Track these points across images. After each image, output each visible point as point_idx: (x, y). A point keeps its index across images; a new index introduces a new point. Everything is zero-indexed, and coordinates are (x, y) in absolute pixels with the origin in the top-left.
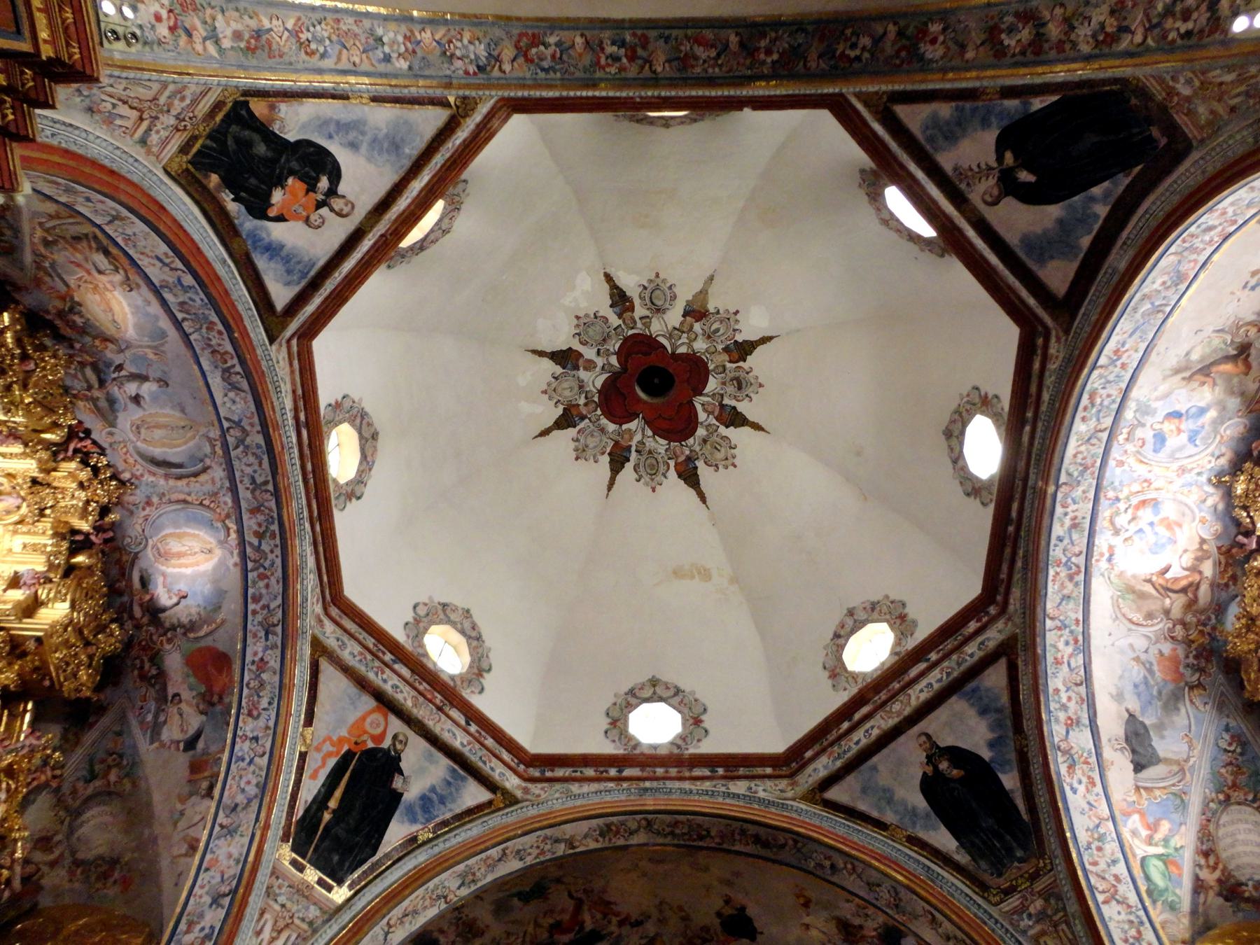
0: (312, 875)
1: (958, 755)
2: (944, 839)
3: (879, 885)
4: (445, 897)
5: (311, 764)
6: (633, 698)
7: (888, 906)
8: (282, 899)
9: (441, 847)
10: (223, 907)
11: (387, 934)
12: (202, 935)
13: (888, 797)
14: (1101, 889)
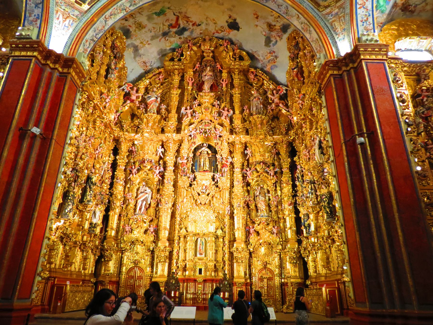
3: (282, 6)
4: (125, 10)
7: (283, 13)
8: (63, 7)
10: (40, 8)
11: (106, 21)
12: (35, 17)
14: (359, 3)
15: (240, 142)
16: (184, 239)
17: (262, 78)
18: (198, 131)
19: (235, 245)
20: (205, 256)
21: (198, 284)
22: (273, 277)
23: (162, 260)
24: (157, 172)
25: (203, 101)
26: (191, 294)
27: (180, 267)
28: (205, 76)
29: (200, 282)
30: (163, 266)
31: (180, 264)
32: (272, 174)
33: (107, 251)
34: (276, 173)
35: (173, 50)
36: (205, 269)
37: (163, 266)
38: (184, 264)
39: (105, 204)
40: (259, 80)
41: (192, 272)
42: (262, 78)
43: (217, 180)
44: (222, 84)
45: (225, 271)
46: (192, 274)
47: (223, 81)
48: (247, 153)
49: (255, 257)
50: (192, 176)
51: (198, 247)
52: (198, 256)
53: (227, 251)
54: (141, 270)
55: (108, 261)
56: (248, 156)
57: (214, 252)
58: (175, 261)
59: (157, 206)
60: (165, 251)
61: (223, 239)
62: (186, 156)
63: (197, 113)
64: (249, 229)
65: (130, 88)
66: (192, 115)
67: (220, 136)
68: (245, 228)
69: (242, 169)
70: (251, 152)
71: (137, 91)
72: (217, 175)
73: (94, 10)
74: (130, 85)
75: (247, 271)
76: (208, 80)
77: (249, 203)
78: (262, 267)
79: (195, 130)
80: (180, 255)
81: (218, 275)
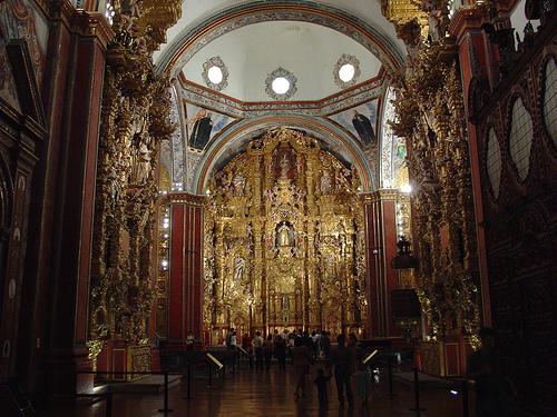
0: (196, 150)
1: (362, 117)
2: (356, 134)
5: (189, 125)
6: (274, 76)
9: (225, 135)
13: (344, 121)
35: (255, 138)
72: (295, 249)
73: (208, 154)
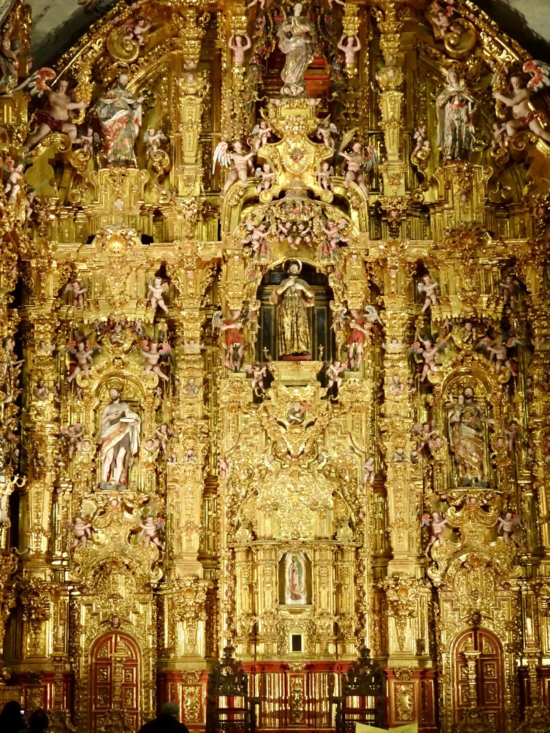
15: (403, 260)
16: (247, 556)
17: (476, 27)
18: (273, 229)
19: (391, 569)
20: (309, 602)
21: (291, 677)
22: (497, 655)
23: (188, 616)
24: (154, 358)
25: (281, 126)
26: (274, 701)
27: (239, 631)
28: (289, 35)
29: (297, 671)
30: (192, 629)
31: (238, 624)
32: (499, 357)
33: (37, 595)
34: (511, 352)
36: (310, 637)
37: (192, 629)
38: (252, 624)
39: (13, 463)
40: (465, 31)
41: (275, 645)
42: (476, 27)
43: (335, 383)
44: (342, 53)
45: (363, 641)
46: (275, 651)
47: (345, 43)
48: (424, 293)
49: (446, 601)
50: (259, 373)
51: (287, 577)
52: (289, 601)
53: (367, 587)
54: (131, 641)
55: (38, 621)
56: (427, 301)
57: (332, 589)
58: (225, 616)
59: (160, 459)
60: (197, 592)
61: (357, 554)
62: (237, 307)
63: (266, 167)
64: (431, 523)
65: (49, 83)
66: (249, 174)
67: (341, 244)
68: (419, 517)
69: (410, 340)
70: (437, 290)
71: (71, 96)
74: (48, 74)
75: (426, 637)
76: (296, 54)
77: (431, 445)
78: (467, 627)
79: (262, 227)
80: (237, 598)
81: (344, 650)
